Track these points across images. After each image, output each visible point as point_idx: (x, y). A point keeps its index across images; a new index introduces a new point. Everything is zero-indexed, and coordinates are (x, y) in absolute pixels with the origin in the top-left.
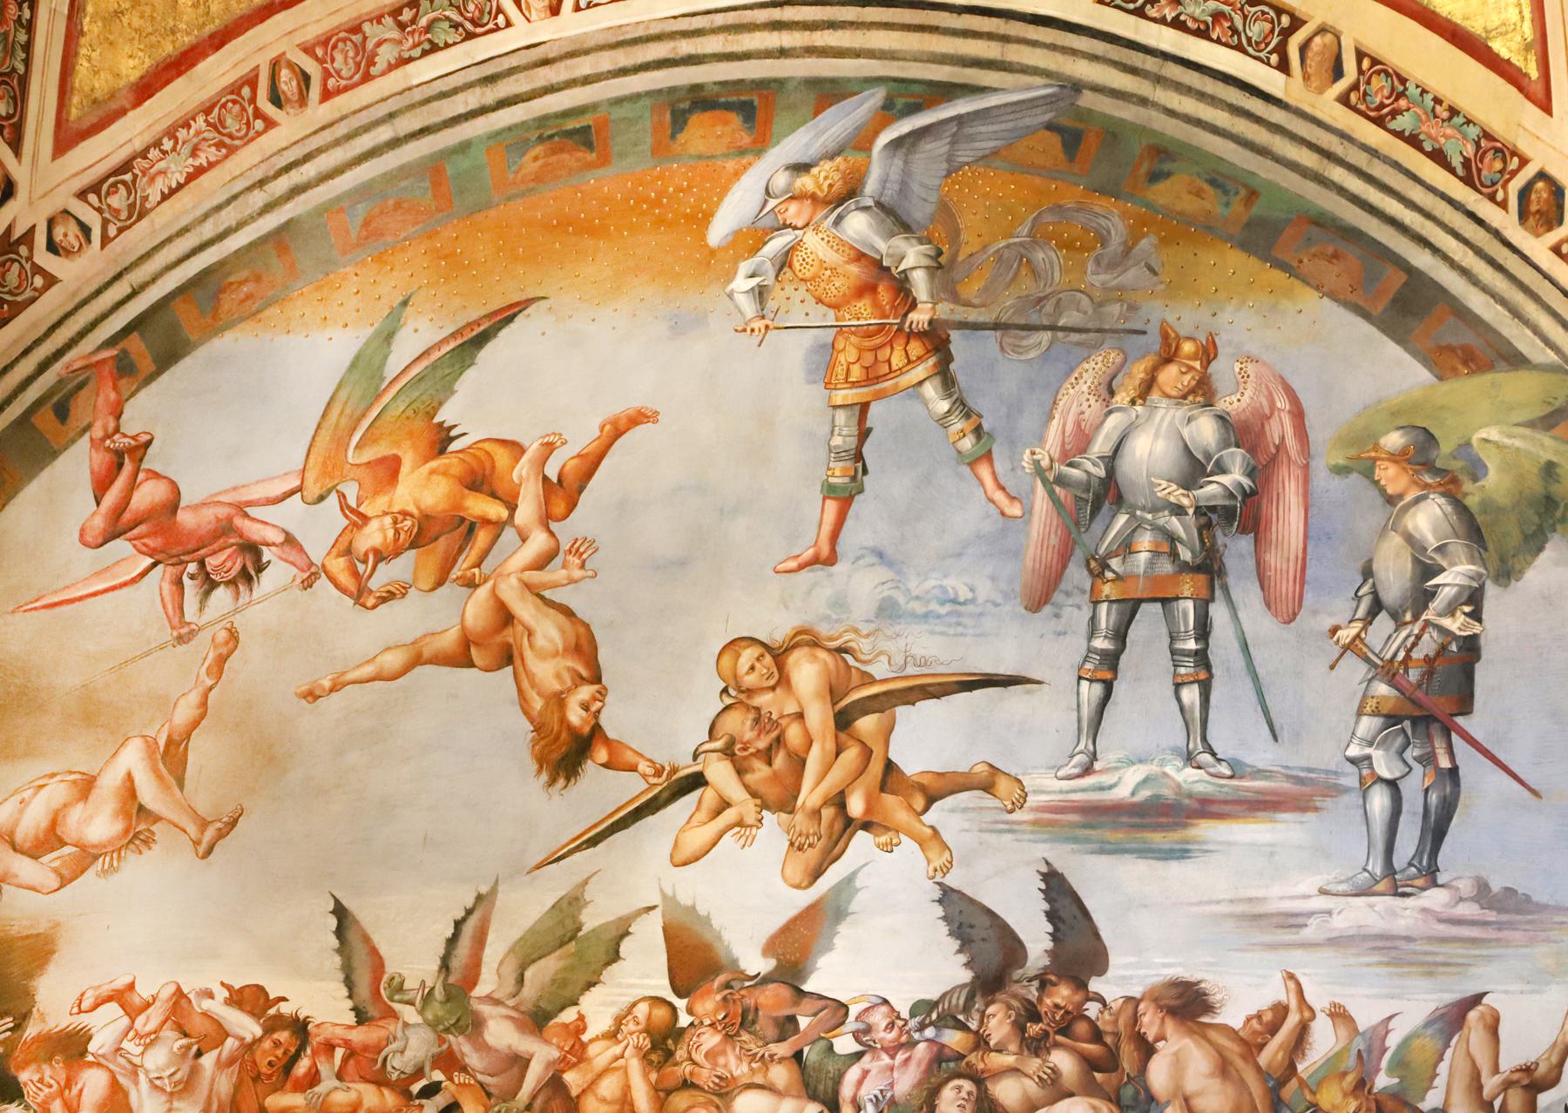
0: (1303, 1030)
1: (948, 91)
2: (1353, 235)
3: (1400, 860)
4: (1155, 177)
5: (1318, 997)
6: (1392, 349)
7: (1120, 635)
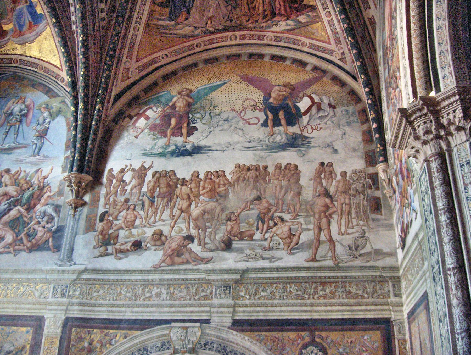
0: (20, 173)
1: (5, 74)
2: (44, 84)
3: (35, 153)
4: (23, 80)
5: (23, 169)
6: (46, 96)
7: (9, 130)
